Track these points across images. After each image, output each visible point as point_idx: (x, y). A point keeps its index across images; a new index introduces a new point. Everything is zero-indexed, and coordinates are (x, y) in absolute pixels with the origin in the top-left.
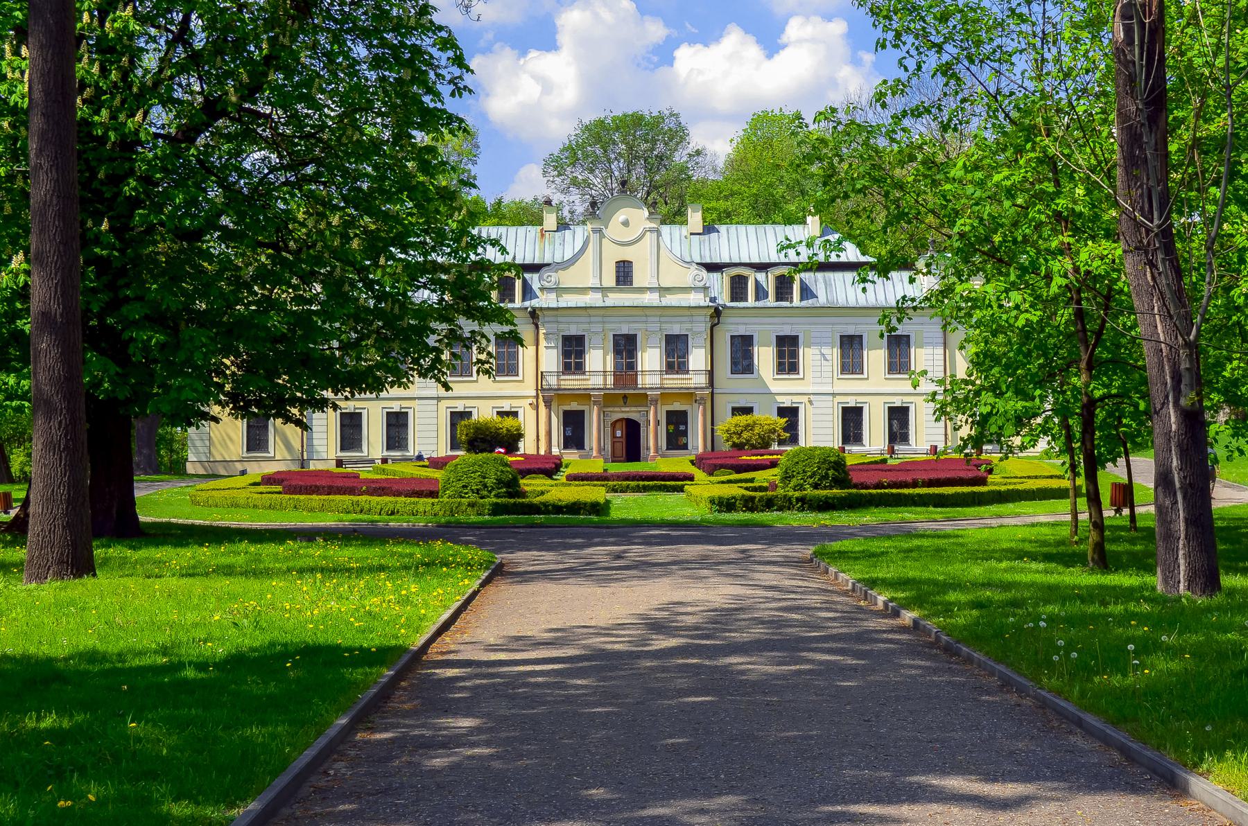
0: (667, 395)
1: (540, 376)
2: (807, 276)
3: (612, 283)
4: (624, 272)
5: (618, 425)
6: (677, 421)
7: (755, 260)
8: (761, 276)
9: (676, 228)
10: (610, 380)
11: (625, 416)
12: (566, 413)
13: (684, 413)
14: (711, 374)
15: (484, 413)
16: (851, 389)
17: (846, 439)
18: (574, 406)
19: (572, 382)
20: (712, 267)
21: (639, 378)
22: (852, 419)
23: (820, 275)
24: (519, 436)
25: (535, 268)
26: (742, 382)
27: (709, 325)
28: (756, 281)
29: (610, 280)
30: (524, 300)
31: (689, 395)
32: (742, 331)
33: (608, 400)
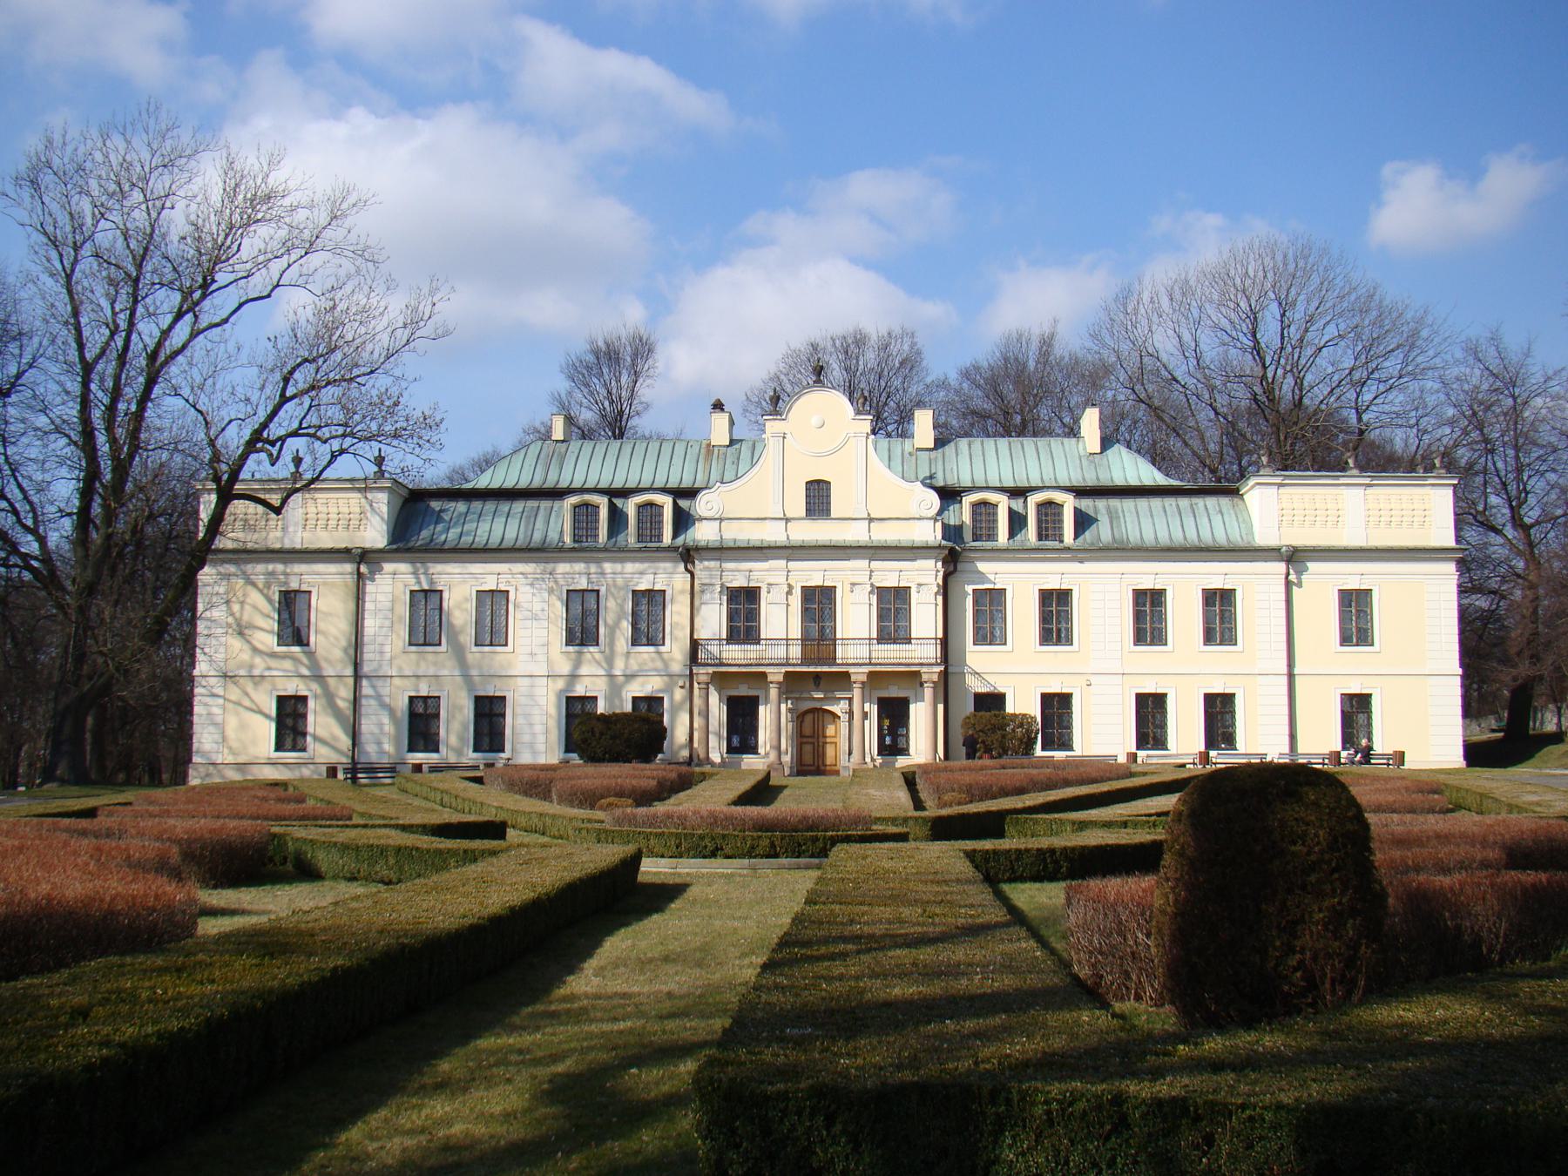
1: (695, 644)
2: (1086, 504)
4: (818, 497)
5: (809, 718)
6: (894, 715)
7: (1009, 483)
8: (1017, 505)
10: (796, 652)
14: (945, 643)
16: (1152, 669)
17: (1142, 741)
21: (839, 648)
22: (1150, 710)
25: (691, 493)
27: (941, 575)
28: (1011, 512)
29: (798, 505)
30: (675, 536)
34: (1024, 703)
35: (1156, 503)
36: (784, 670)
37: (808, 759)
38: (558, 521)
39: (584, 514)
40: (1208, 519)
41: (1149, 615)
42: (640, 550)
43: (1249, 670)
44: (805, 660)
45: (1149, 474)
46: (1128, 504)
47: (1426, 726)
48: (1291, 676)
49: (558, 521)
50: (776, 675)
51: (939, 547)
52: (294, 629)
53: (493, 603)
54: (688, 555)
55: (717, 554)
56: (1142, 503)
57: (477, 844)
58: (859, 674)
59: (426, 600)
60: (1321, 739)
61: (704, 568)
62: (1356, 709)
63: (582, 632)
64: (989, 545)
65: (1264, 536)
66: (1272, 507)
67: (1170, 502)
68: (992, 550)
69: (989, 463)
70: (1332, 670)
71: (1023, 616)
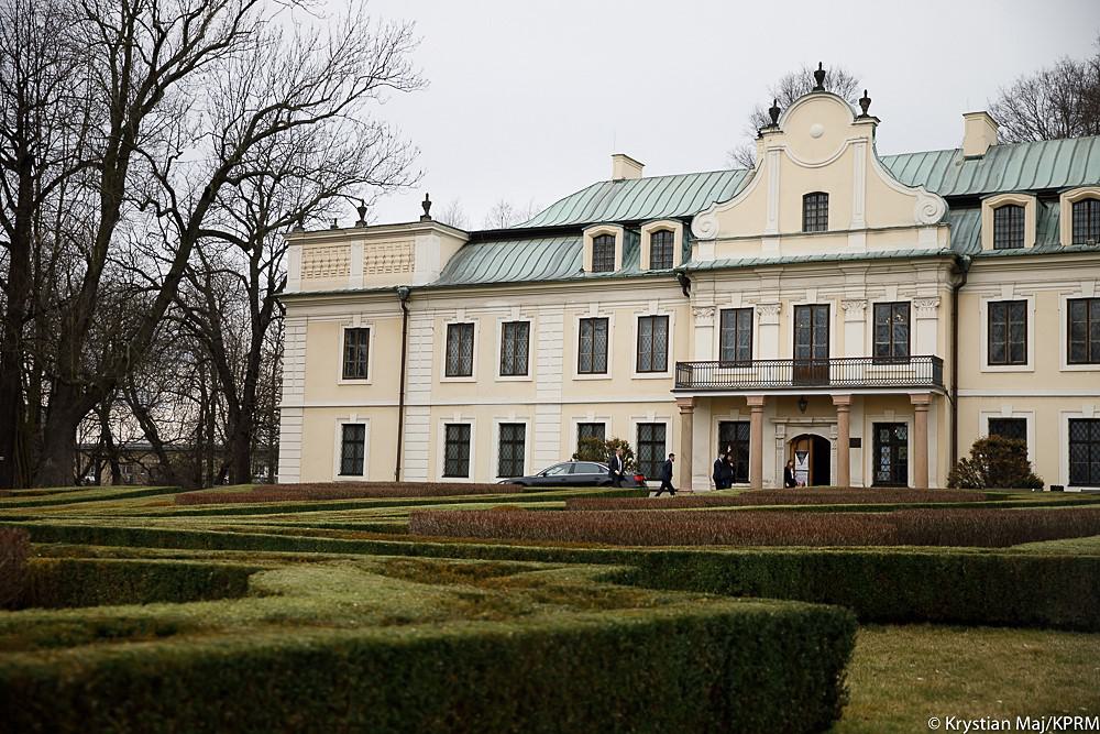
0: (865, 402)
3: (800, 229)
6: (890, 442)
11: (809, 432)
12: (722, 425)
18: (734, 417)
26: (1008, 380)
32: (1007, 294)
33: (778, 404)
38: (582, 254)
39: (603, 244)
49: (582, 254)
50: (755, 398)
52: (355, 365)
53: (517, 332)
54: (685, 279)
55: (709, 276)
58: (840, 397)
59: (461, 335)
61: (702, 291)
63: (592, 359)
64: (1020, 251)
68: (1008, 257)
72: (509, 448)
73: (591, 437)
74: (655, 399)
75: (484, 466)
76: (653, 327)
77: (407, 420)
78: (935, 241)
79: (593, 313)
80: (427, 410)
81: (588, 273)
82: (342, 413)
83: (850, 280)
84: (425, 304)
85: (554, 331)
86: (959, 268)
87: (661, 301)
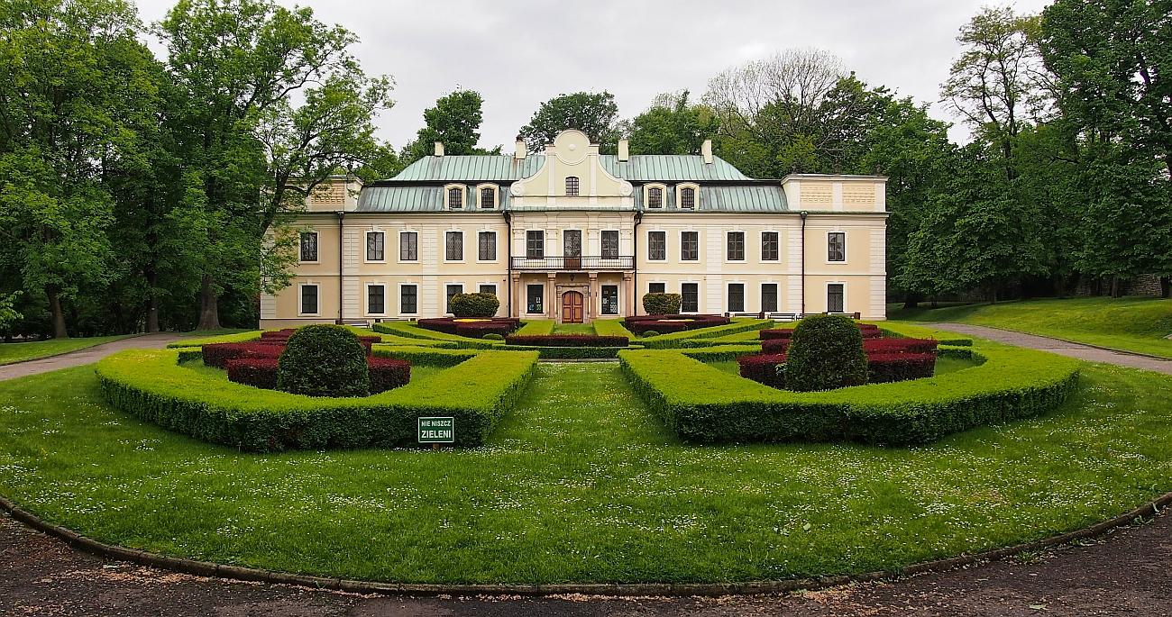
1: (511, 259)
2: (704, 189)
4: (572, 185)
5: (568, 295)
6: (610, 293)
9: (609, 157)
10: (562, 263)
13: (616, 287)
15: (471, 288)
18: (535, 282)
19: (535, 264)
20: (635, 183)
22: (736, 293)
23: (712, 190)
24: (496, 305)
25: (508, 183)
31: (619, 275)
34: (674, 288)
35: (740, 189)
36: (556, 272)
37: (567, 316)
39: (455, 195)
40: (764, 197)
41: (736, 246)
42: (483, 212)
43: (784, 272)
44: (566, 267)
45: (733, 174)
46: (725, 191)
47: (867, 301)
48: (803, 275)
50: (552, 274)
51: (633, 211)
54: (507, 216)
55: (520, 214)
56: (733, 189)
57: (637, 346)
58: (593, 274)
60: (819, 306)
62: (835, 292)
65: (794, 205)
66: (798, 192)
67: (746, 189)
69: (658, 167)
70: (824, 272)
71: (673, 245)
72: (406, 299)
73: (454, 290)
74: (492, 274)
75: (393, 306)
76: (487, 237)
77: (344, 283)
78: (628, 204)
79: (455, 229)
80: (357, 278)
81: (447, 208)
82: (370, 279)
83: (590, 219)
84: (353, 221)
85: (432, 238)
86: (638, 216)
87: (494, 225)
